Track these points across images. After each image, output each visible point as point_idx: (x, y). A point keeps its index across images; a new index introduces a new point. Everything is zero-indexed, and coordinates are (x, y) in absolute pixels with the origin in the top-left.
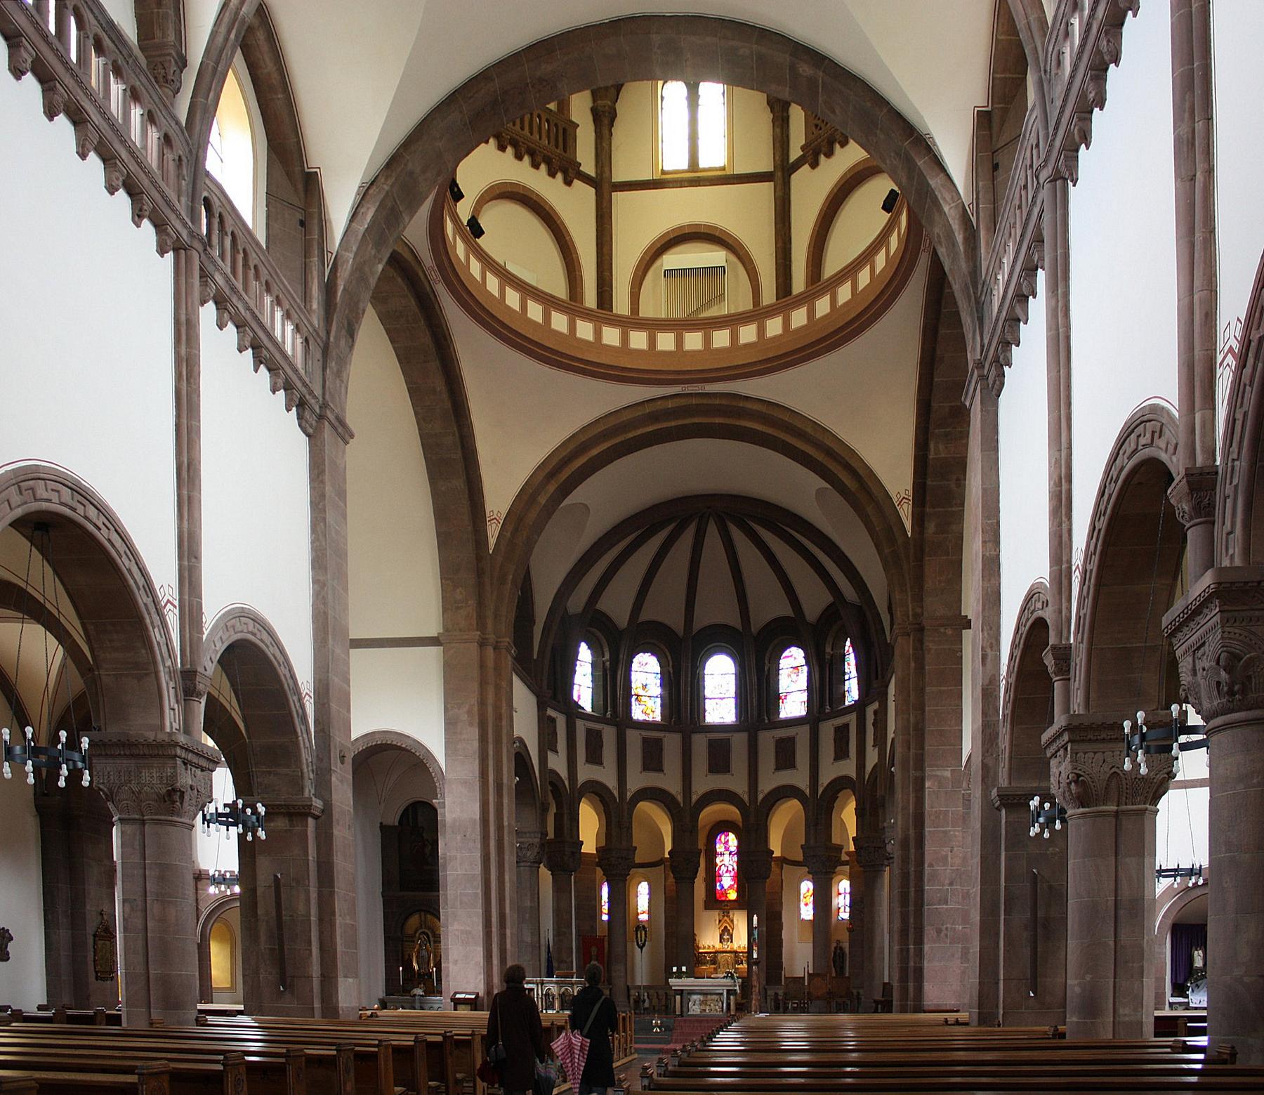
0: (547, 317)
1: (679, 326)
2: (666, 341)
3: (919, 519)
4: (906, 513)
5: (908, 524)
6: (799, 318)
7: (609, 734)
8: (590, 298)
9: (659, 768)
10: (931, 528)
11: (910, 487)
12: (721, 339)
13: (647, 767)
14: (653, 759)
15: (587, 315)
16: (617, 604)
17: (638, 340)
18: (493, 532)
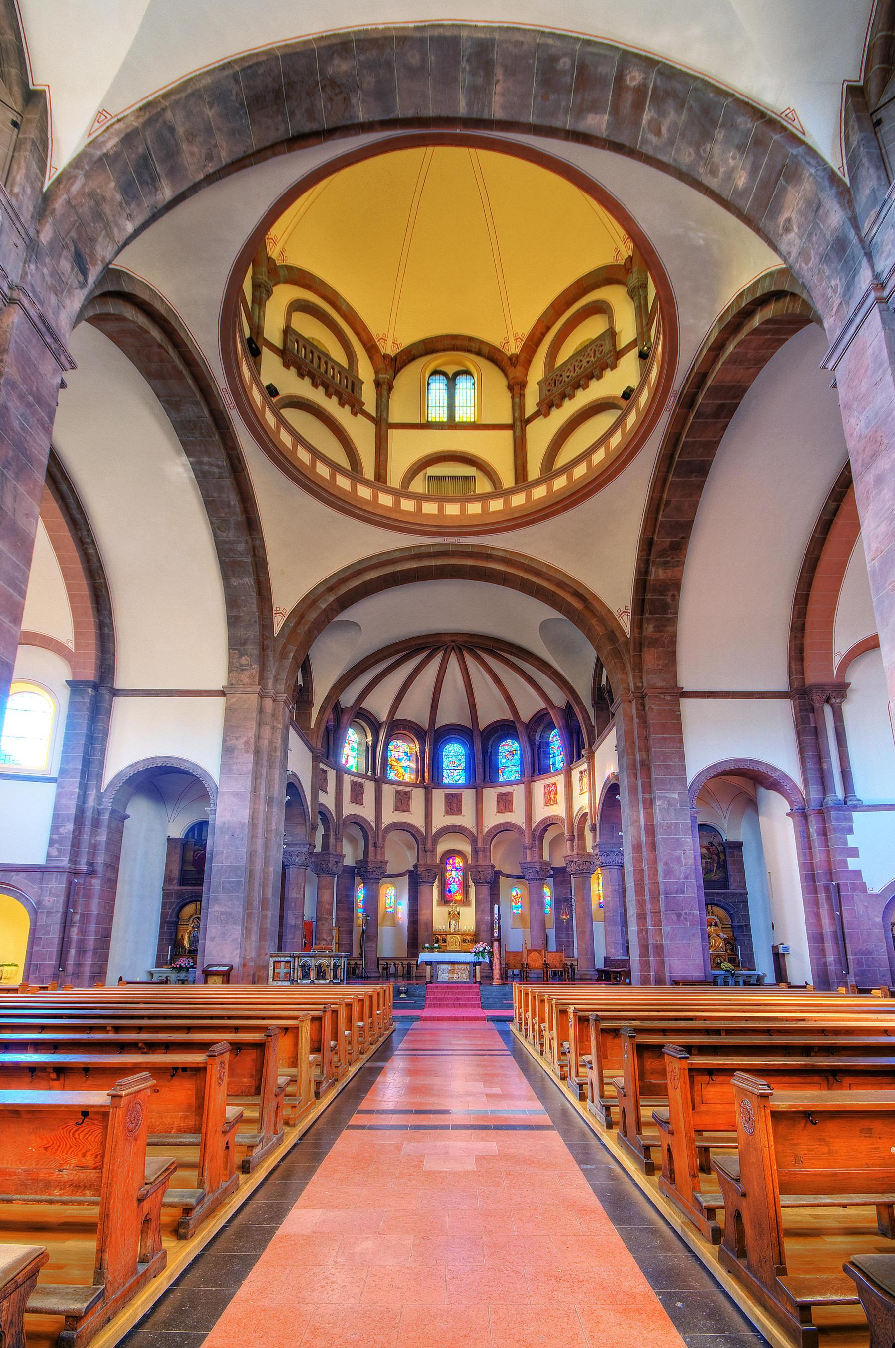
13: (397, 809)
17: (407, 505)
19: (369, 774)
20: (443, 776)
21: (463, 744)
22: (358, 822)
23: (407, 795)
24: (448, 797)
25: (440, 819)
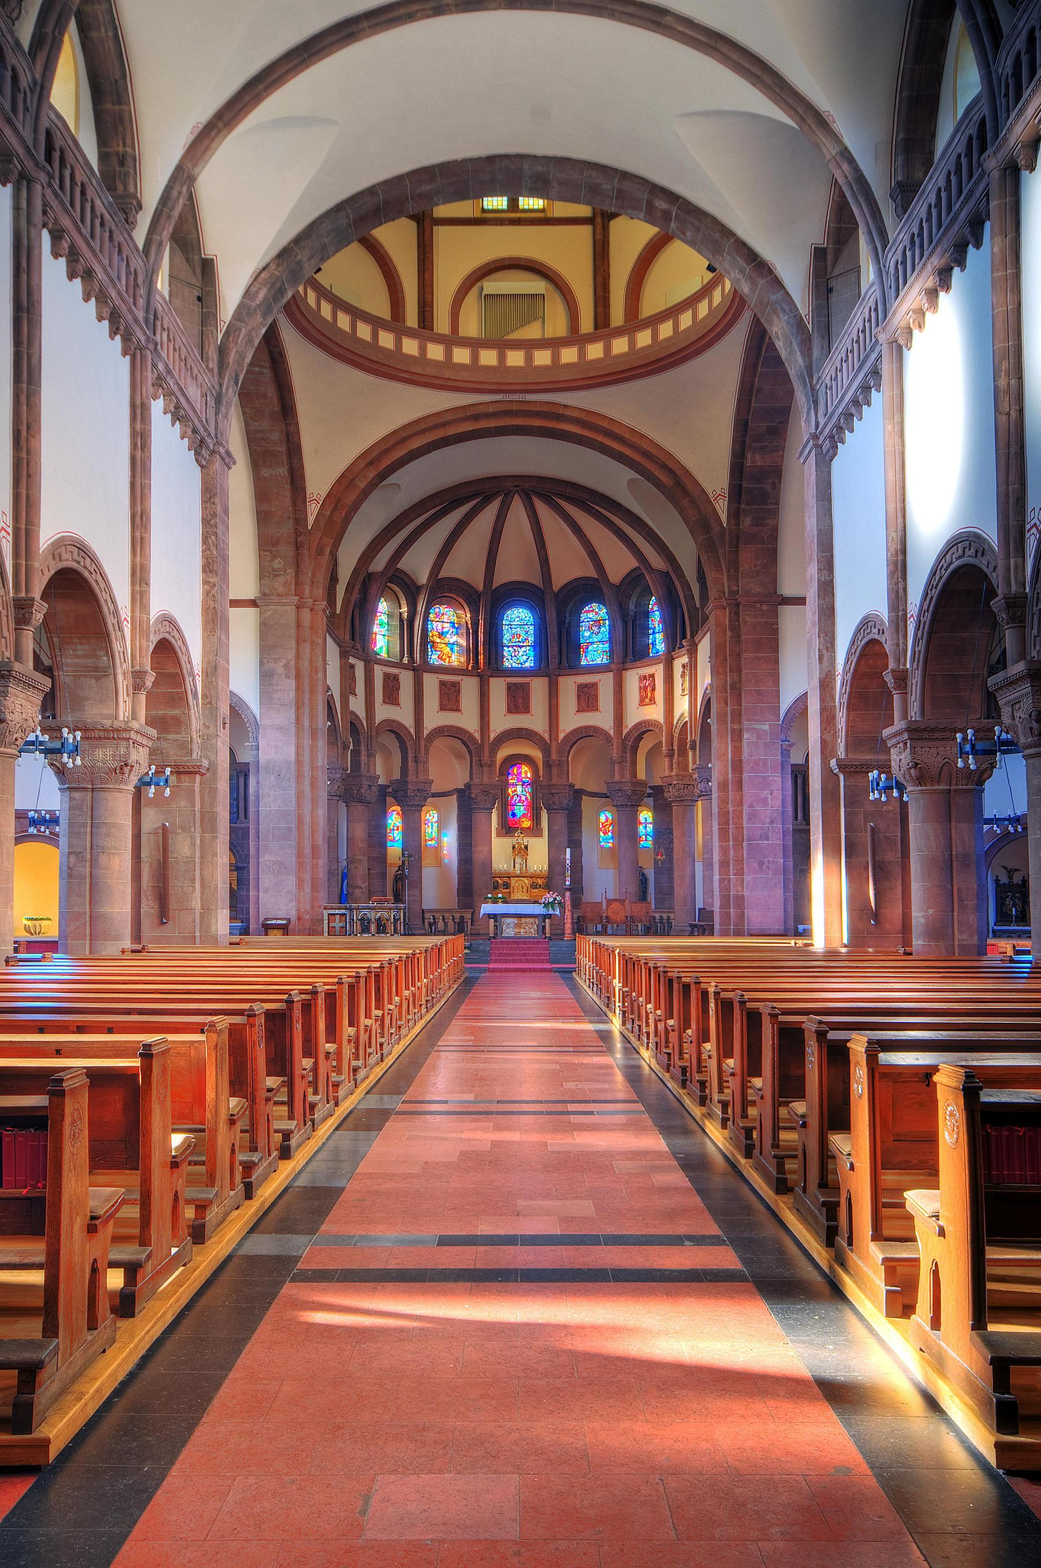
0: (375, 336)
1: (503, 345)
2: (488, 358)
6: (620, 346)
7: (406, 679)
8: (412, 319)
11: (726, 486)
12: (542, 358)
13: (443, 707)
15: (411, 333)
16: (419, 564)
17: (461, 356)
18: (313, 510)
19: (405, 660)
20: (503, 657)
21: (530, 608)
23: (456, 686)
25: (501, 721)
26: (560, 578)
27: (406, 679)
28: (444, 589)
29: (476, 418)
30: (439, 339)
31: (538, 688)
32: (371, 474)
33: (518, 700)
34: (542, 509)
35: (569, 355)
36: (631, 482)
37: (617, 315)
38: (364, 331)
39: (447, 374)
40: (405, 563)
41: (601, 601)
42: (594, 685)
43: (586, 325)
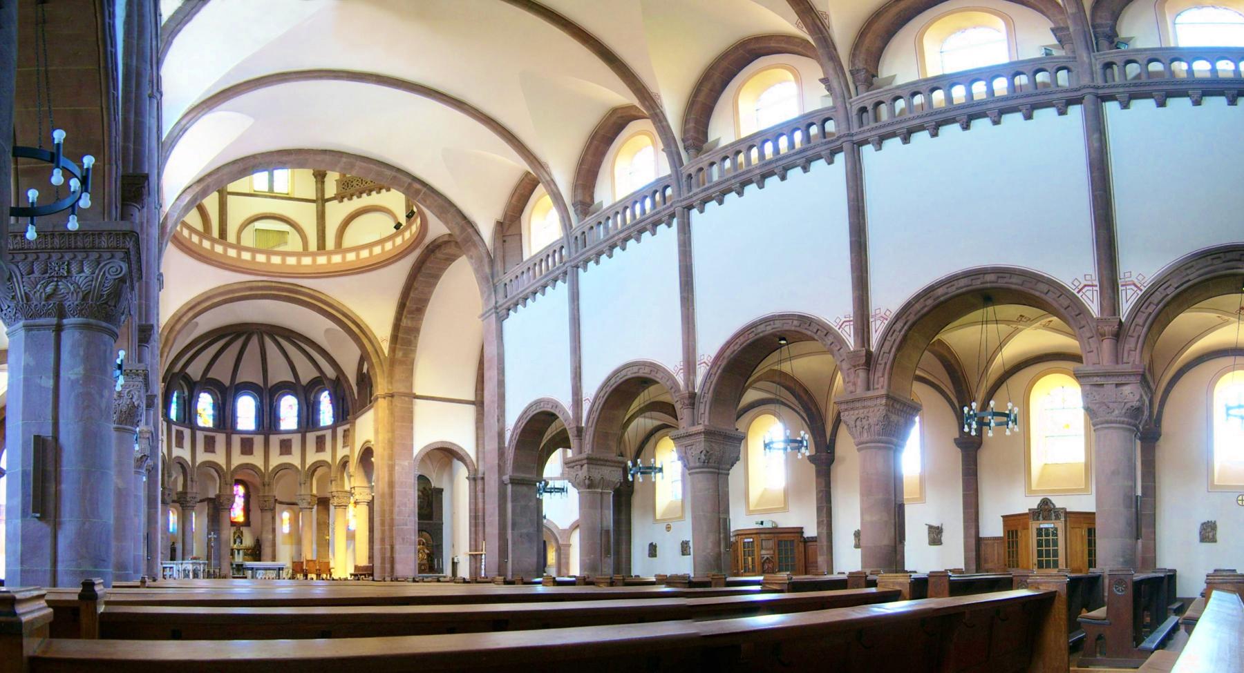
1: (269, 253)
2: (261, 258)
3: (393, 350)
4: (385, 347)
5: (386, 352)
9: (213, 452)
10: (399, 354)
13: (207, 450)
14: (210, 445)
17: (246, 256)
22: (181, 463)
24: (242, 440)
26: (274, 379)
27: (187, 432)
28: (209, 384)
29: (251, 289)
30: (232, 246)
31: (259, 440)
32: (190, 314)
33: (247, 447)
34: (269, 343)
35: (307, 261)
36: (327, 331)
37: (330, 243)
38: (195, 239)
39: (238, 264)
40: (189, 370)
41: (296, 394)
42: (289, 441)
43: (313, 246)
